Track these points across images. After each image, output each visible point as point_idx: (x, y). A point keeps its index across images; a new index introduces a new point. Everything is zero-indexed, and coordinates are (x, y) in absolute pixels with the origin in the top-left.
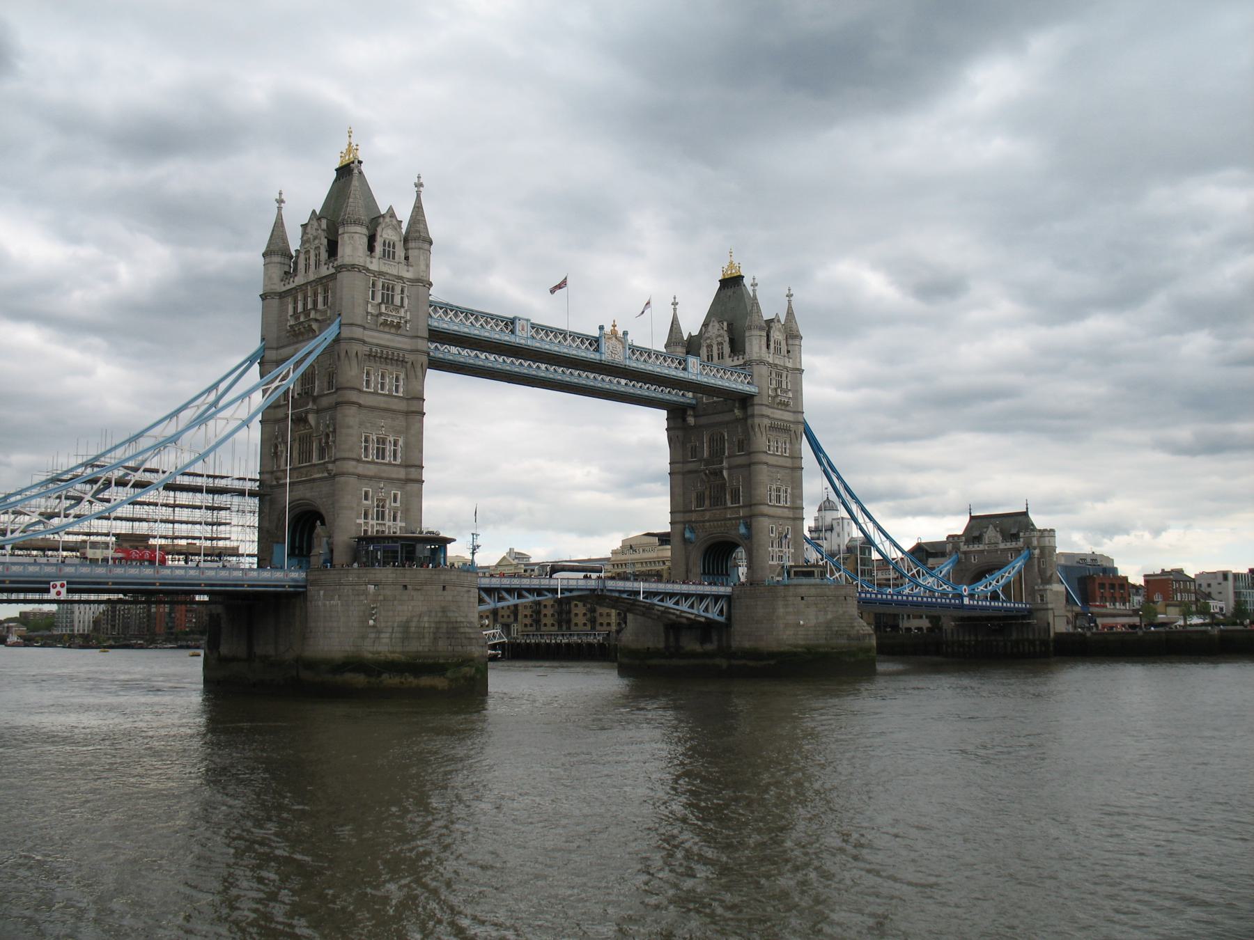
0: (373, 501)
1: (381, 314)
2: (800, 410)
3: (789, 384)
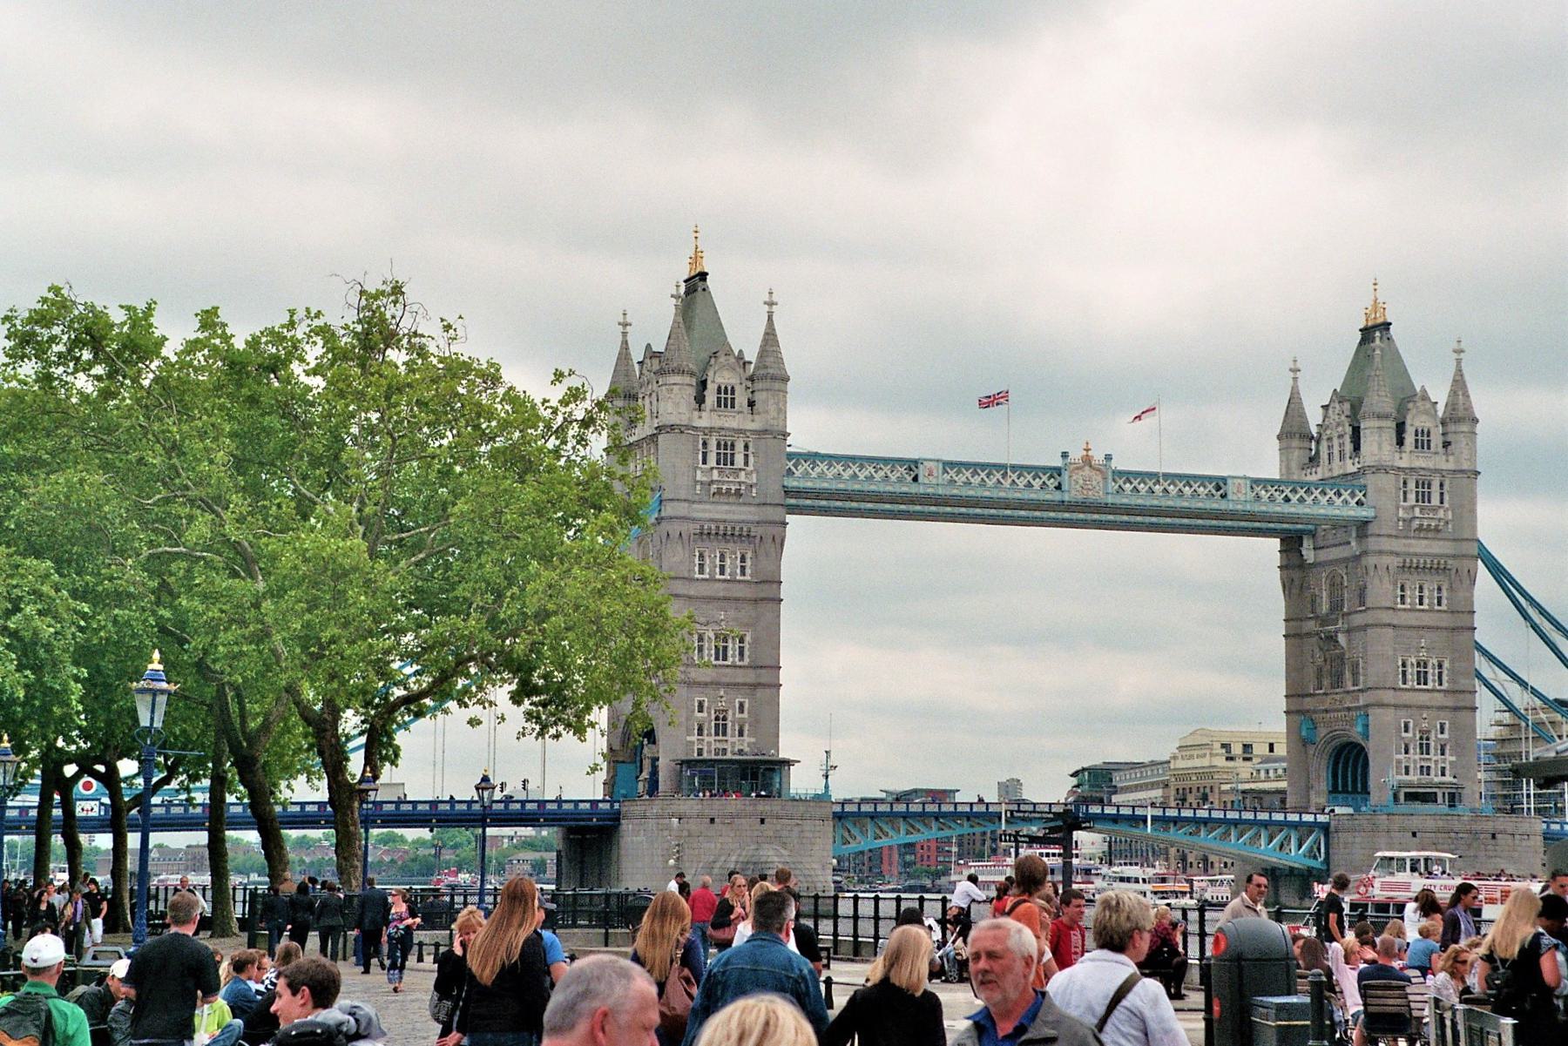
0: (709, 713)
1: (712, 482)
2: (1466, 536)
3: (1446, 497)
